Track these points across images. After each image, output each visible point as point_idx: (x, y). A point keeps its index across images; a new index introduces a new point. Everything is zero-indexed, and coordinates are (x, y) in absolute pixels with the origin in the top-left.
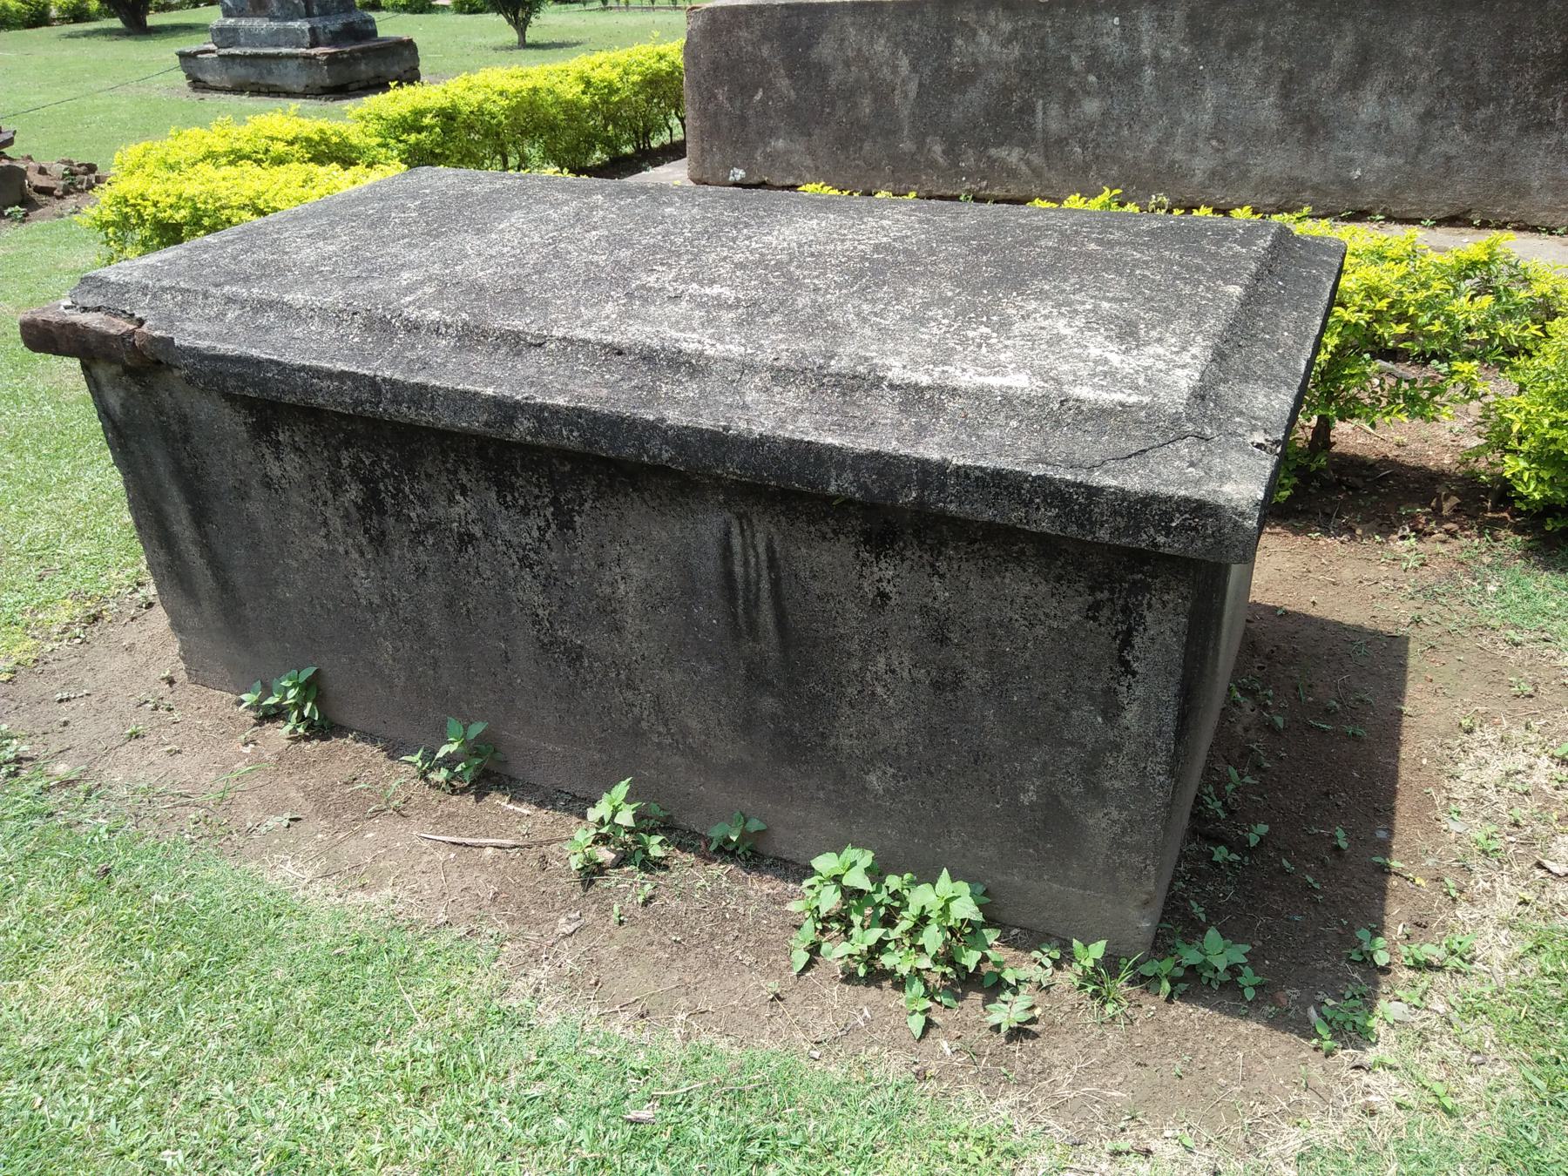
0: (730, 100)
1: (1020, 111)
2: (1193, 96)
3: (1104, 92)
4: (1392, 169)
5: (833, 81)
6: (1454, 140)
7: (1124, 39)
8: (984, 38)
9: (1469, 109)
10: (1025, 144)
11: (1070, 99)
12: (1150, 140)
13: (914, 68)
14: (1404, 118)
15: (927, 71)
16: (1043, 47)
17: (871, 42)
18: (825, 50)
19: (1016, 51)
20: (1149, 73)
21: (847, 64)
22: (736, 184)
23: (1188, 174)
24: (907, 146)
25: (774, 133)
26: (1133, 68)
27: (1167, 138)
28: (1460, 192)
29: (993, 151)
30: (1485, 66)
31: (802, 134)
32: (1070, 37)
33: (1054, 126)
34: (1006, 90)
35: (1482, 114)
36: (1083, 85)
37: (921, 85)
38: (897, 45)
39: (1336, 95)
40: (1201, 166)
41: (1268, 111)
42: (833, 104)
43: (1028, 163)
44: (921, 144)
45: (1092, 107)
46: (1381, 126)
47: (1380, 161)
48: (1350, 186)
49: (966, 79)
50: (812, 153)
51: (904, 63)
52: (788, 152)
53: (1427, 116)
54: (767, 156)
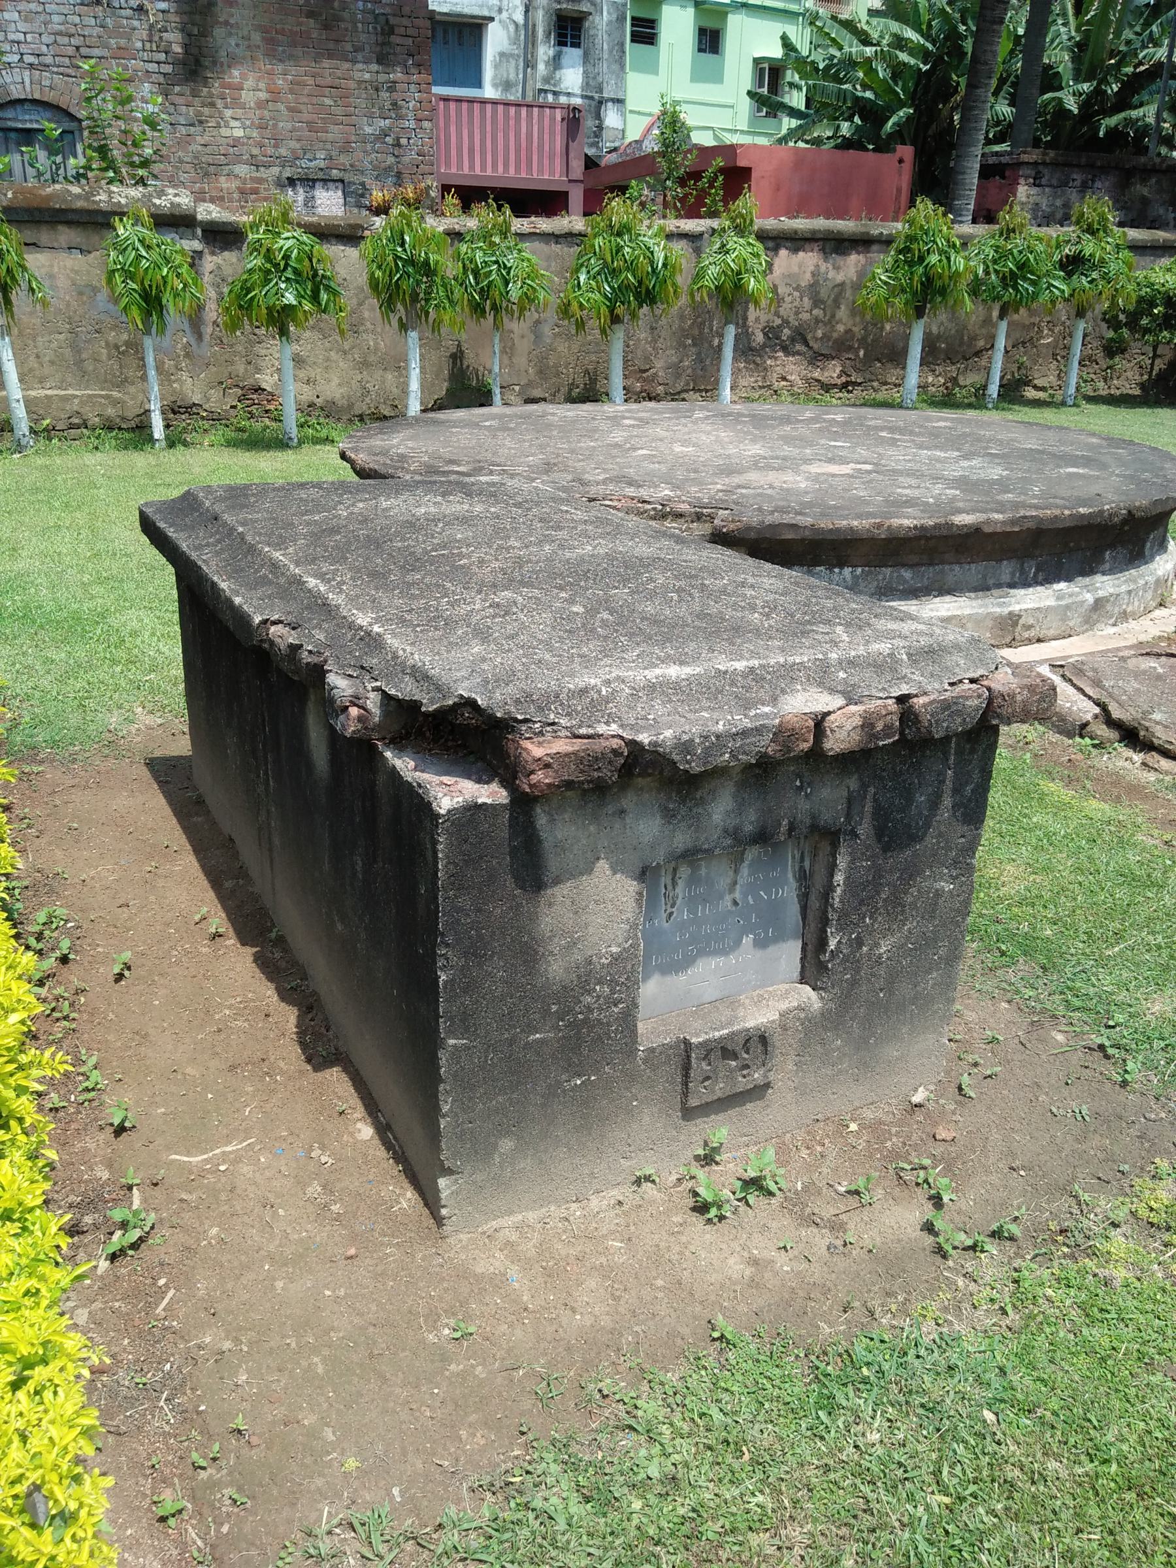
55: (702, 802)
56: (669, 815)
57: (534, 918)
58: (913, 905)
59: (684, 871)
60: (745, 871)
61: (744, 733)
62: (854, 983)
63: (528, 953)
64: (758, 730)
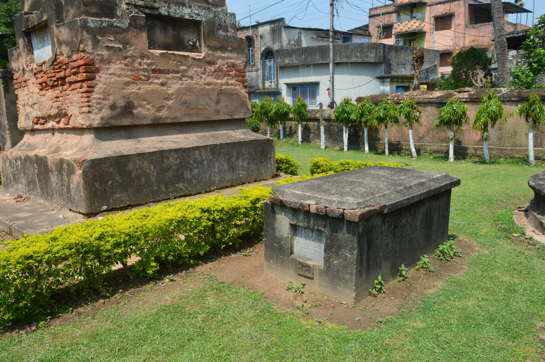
0: (100, 186)
1: (181, 174)
2: (214, 165)
3: (197, 168)
4: (245, 174)
5: (133, 175)
6: (252, 167)
7: (200, 155)
8: (171, 159)
9: (253, 161)
10: (183, 182)
11: (191, 170)
12: (208, 176)
13: (155, 168)
14: (245, 164)
15: (158, 168)
16: (184, 159)
17: (143, 163)
18: (130, 167)
19: (178, 161)
20: (205, 162)
21: (137, 170)
22: (104, 211)
23: (215, 182)
24: (155, 188)
25: (116, 193)
26: (202, 161)
27: (210, 175)
28: (254, 176)
29: (176, 185)
30: (254, 153)
31: (125, 191)
32: (189, 156)
33: (189, 177)
34: (177, 170)
35: (255, 161)
36: (193, 166)
37: (157, 172)
38: (150, 163)
39: (235, 162)
40: (217, 179)
41: (226, 167)
42: (133, 181)
43: (184, 186)
44: (159, 187)
45: (196, 171)
46: (242, 166)
47: (244, 173)
48: (240, 178)
49: (168, 169)
50: (129, 196)
51: (152, 167)
52: (121, 197)
53: (248, 163)
54: (114, 200)
55: (298, 215)
56: (293, 216)
57: (274, 224)
58: (341, 256)
59: (303, 230)
60: (314, 235)
61: (295, 203)
62: (329, 267)
63: (274, 230)
64: (297, 203)
